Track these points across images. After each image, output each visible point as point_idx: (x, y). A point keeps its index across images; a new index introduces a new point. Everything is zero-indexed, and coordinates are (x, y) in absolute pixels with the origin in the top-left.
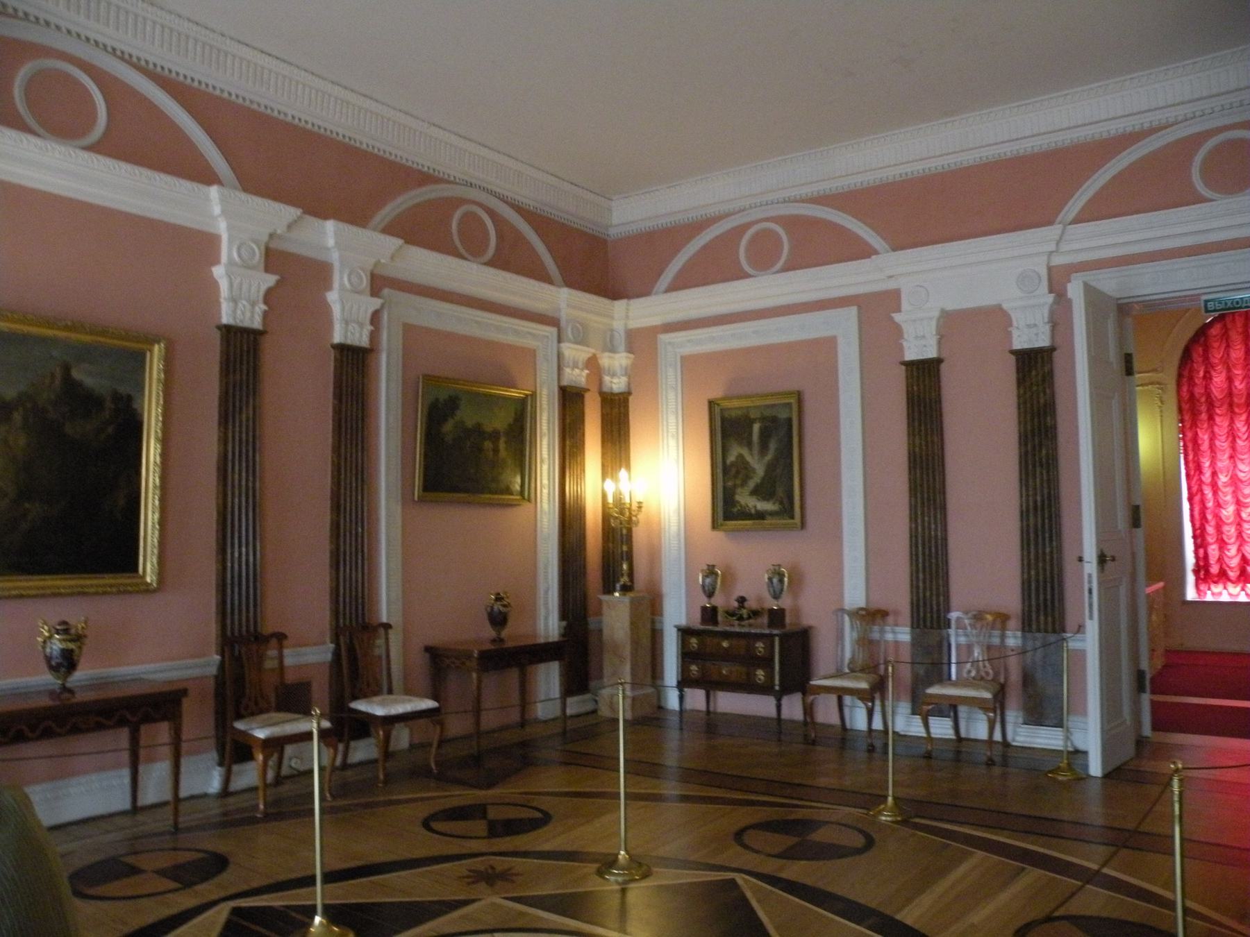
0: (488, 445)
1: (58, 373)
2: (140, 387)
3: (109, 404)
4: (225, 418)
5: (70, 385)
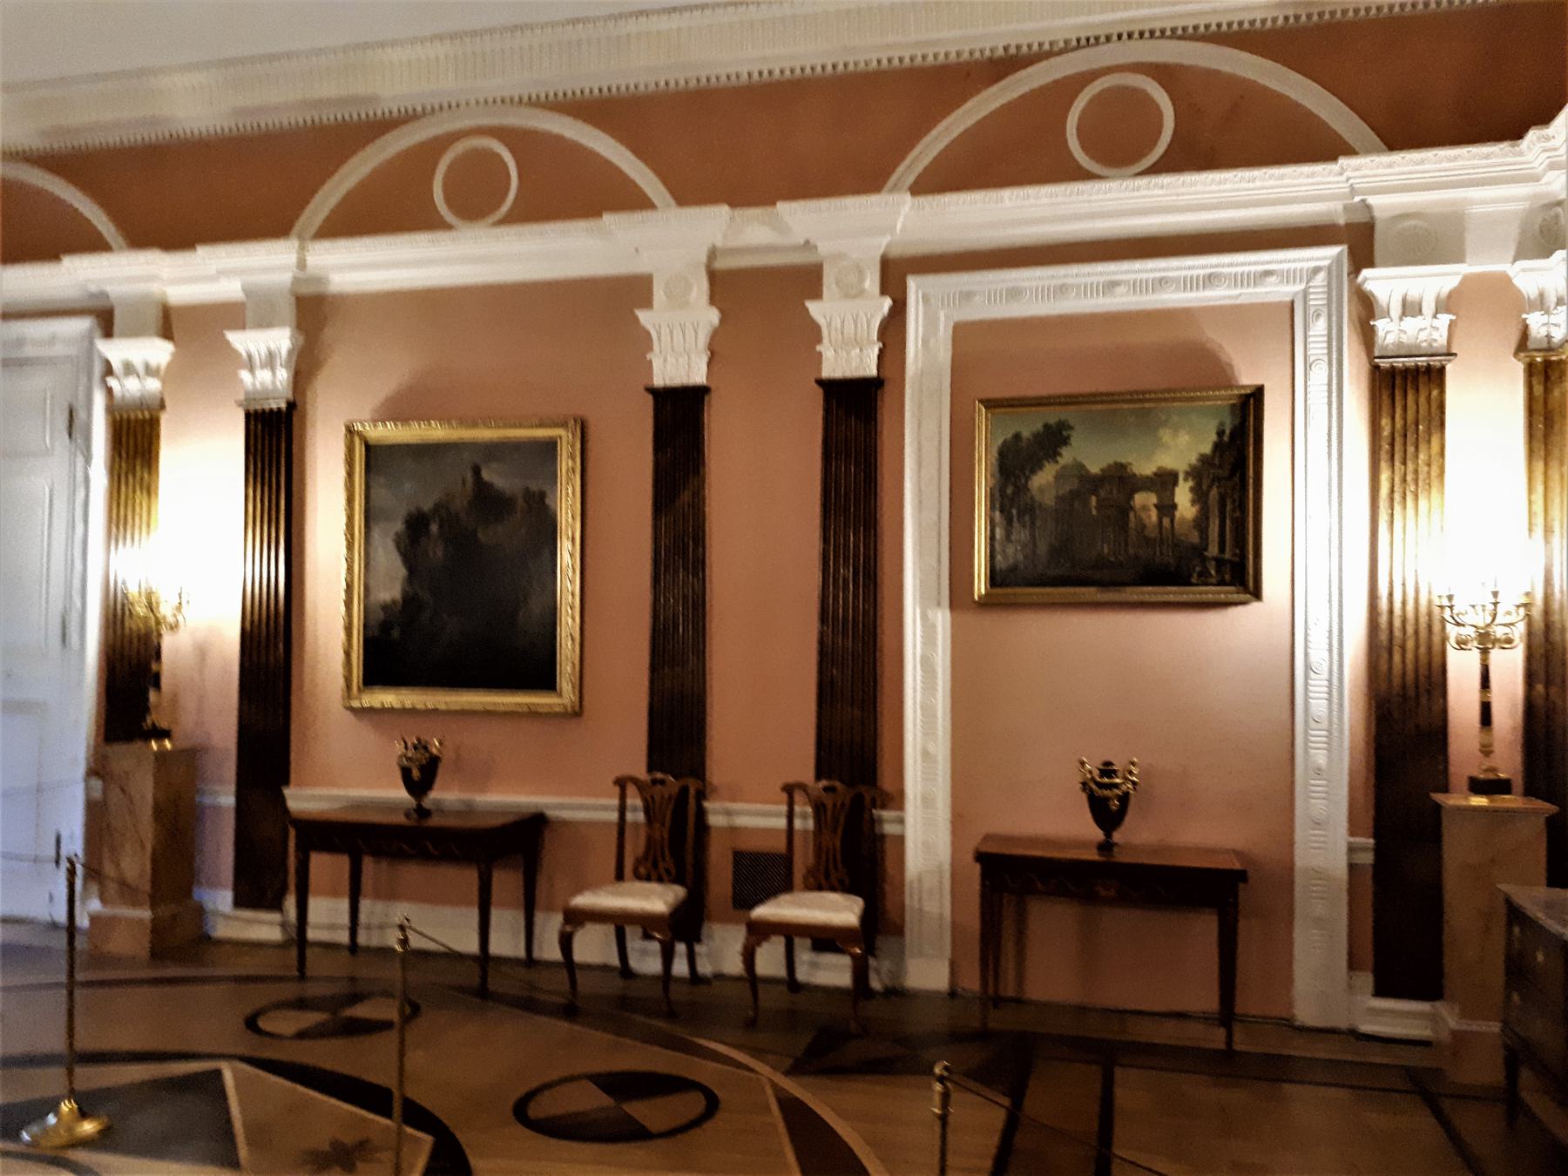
0: (1145, 500)
1: (469, 476)
2: (553, 478)
3: (520, 502)
5: (482, 488)
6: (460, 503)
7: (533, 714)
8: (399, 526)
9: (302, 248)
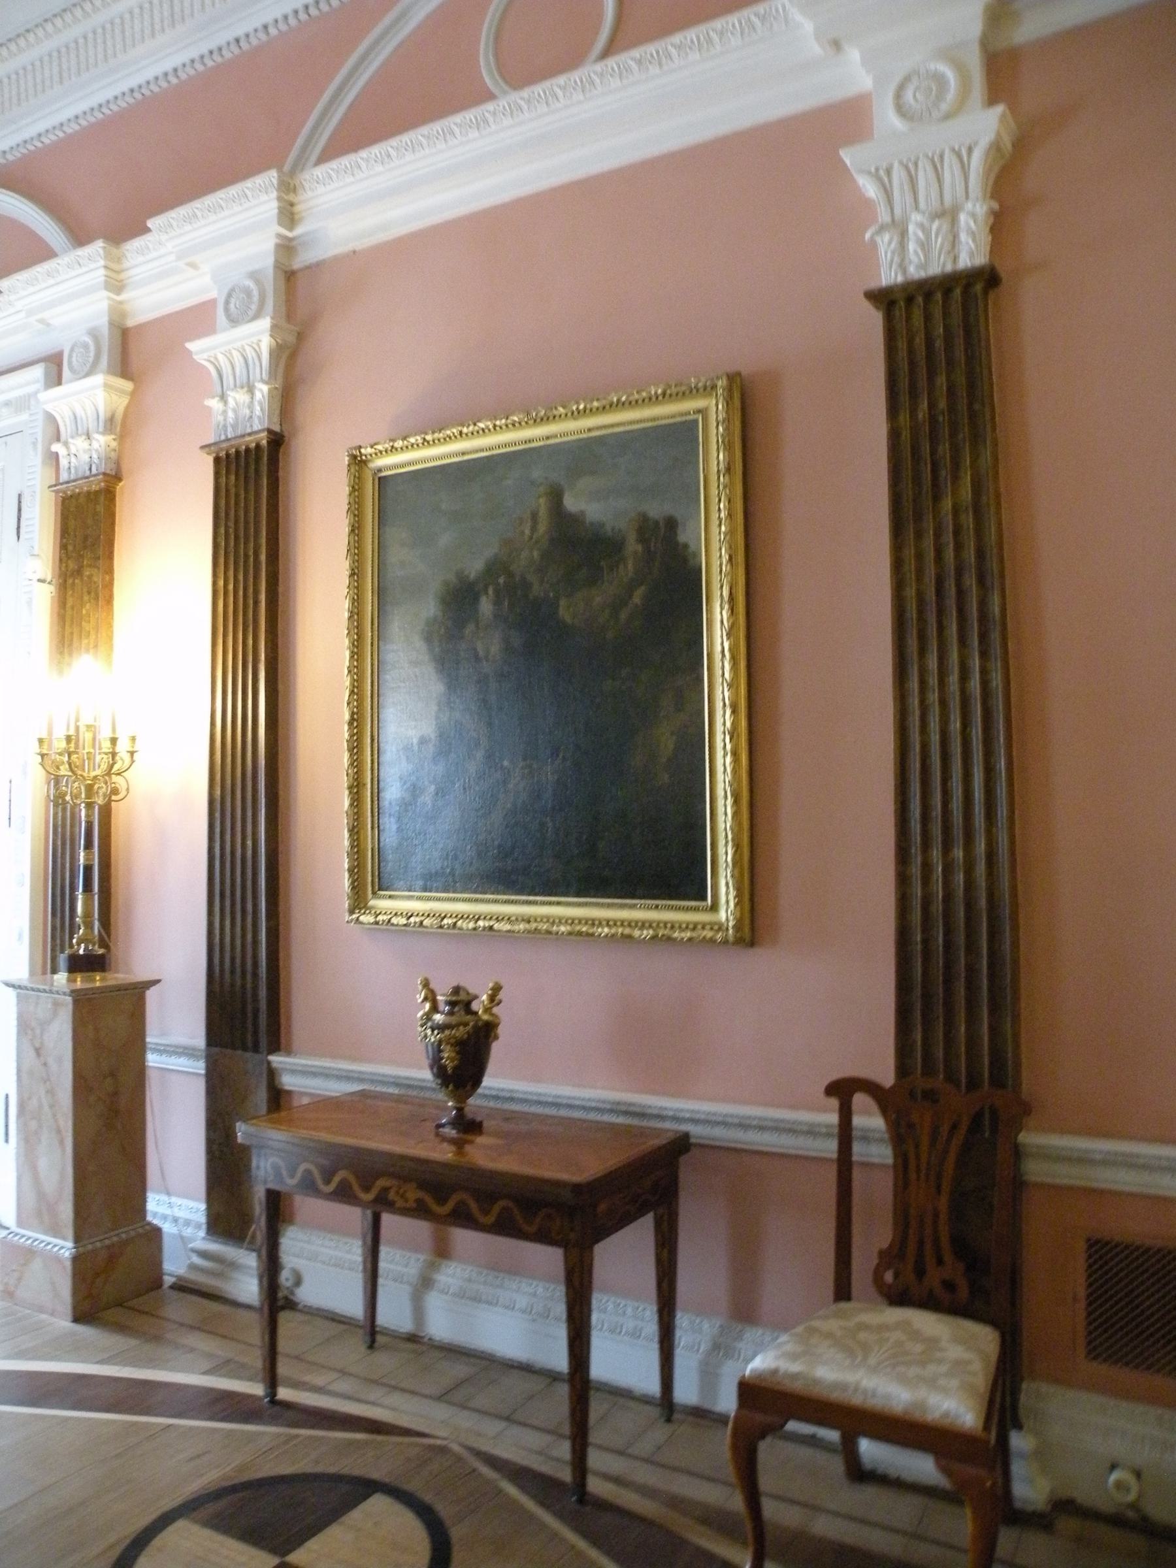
1: (543, 505)
3: (633, 546)
4: (905, 517)
6: (526, 559)
7: (663, 940)
8: (430, 608)
9: (288, 188)
